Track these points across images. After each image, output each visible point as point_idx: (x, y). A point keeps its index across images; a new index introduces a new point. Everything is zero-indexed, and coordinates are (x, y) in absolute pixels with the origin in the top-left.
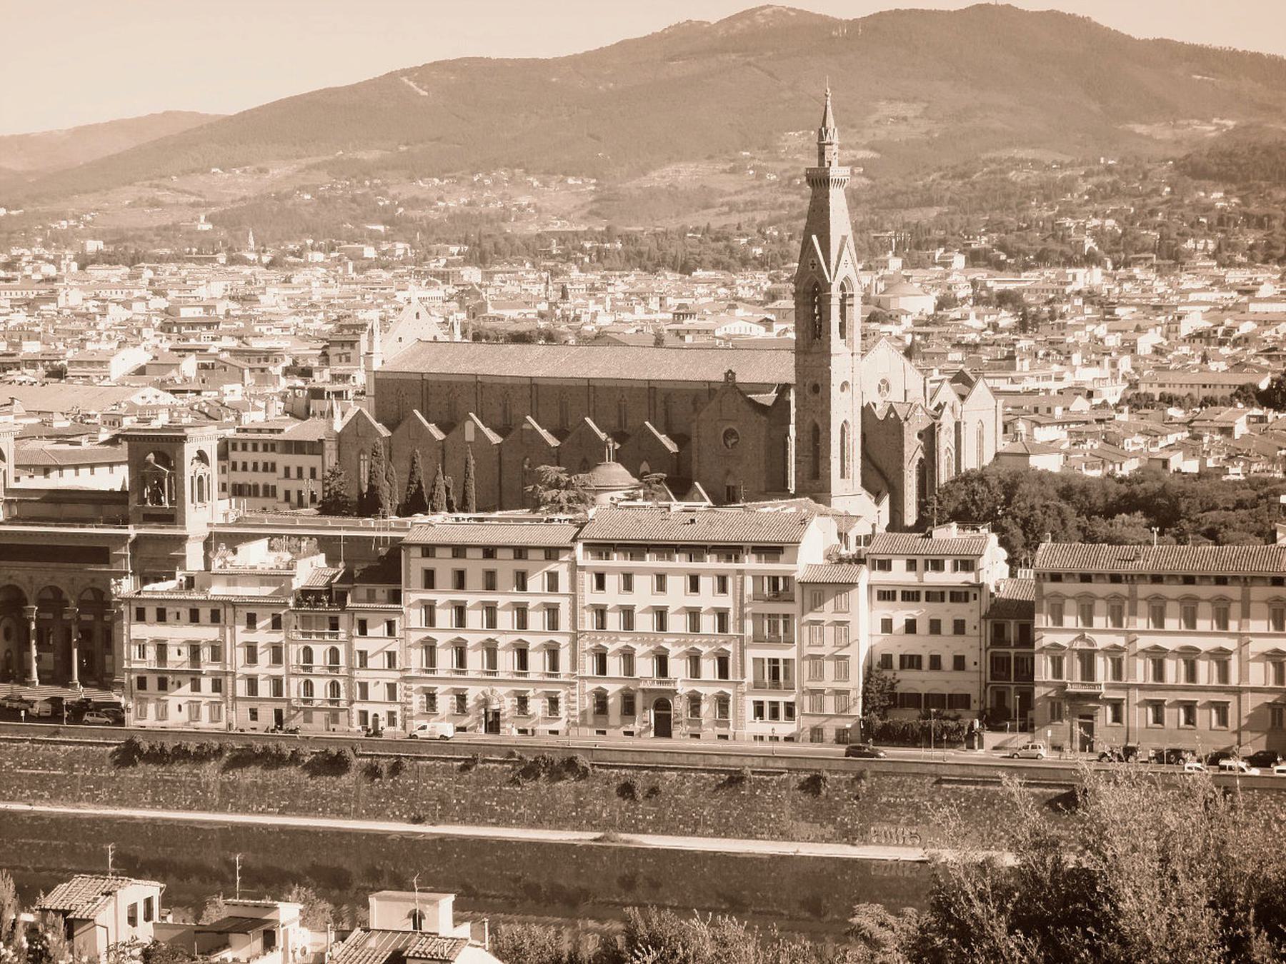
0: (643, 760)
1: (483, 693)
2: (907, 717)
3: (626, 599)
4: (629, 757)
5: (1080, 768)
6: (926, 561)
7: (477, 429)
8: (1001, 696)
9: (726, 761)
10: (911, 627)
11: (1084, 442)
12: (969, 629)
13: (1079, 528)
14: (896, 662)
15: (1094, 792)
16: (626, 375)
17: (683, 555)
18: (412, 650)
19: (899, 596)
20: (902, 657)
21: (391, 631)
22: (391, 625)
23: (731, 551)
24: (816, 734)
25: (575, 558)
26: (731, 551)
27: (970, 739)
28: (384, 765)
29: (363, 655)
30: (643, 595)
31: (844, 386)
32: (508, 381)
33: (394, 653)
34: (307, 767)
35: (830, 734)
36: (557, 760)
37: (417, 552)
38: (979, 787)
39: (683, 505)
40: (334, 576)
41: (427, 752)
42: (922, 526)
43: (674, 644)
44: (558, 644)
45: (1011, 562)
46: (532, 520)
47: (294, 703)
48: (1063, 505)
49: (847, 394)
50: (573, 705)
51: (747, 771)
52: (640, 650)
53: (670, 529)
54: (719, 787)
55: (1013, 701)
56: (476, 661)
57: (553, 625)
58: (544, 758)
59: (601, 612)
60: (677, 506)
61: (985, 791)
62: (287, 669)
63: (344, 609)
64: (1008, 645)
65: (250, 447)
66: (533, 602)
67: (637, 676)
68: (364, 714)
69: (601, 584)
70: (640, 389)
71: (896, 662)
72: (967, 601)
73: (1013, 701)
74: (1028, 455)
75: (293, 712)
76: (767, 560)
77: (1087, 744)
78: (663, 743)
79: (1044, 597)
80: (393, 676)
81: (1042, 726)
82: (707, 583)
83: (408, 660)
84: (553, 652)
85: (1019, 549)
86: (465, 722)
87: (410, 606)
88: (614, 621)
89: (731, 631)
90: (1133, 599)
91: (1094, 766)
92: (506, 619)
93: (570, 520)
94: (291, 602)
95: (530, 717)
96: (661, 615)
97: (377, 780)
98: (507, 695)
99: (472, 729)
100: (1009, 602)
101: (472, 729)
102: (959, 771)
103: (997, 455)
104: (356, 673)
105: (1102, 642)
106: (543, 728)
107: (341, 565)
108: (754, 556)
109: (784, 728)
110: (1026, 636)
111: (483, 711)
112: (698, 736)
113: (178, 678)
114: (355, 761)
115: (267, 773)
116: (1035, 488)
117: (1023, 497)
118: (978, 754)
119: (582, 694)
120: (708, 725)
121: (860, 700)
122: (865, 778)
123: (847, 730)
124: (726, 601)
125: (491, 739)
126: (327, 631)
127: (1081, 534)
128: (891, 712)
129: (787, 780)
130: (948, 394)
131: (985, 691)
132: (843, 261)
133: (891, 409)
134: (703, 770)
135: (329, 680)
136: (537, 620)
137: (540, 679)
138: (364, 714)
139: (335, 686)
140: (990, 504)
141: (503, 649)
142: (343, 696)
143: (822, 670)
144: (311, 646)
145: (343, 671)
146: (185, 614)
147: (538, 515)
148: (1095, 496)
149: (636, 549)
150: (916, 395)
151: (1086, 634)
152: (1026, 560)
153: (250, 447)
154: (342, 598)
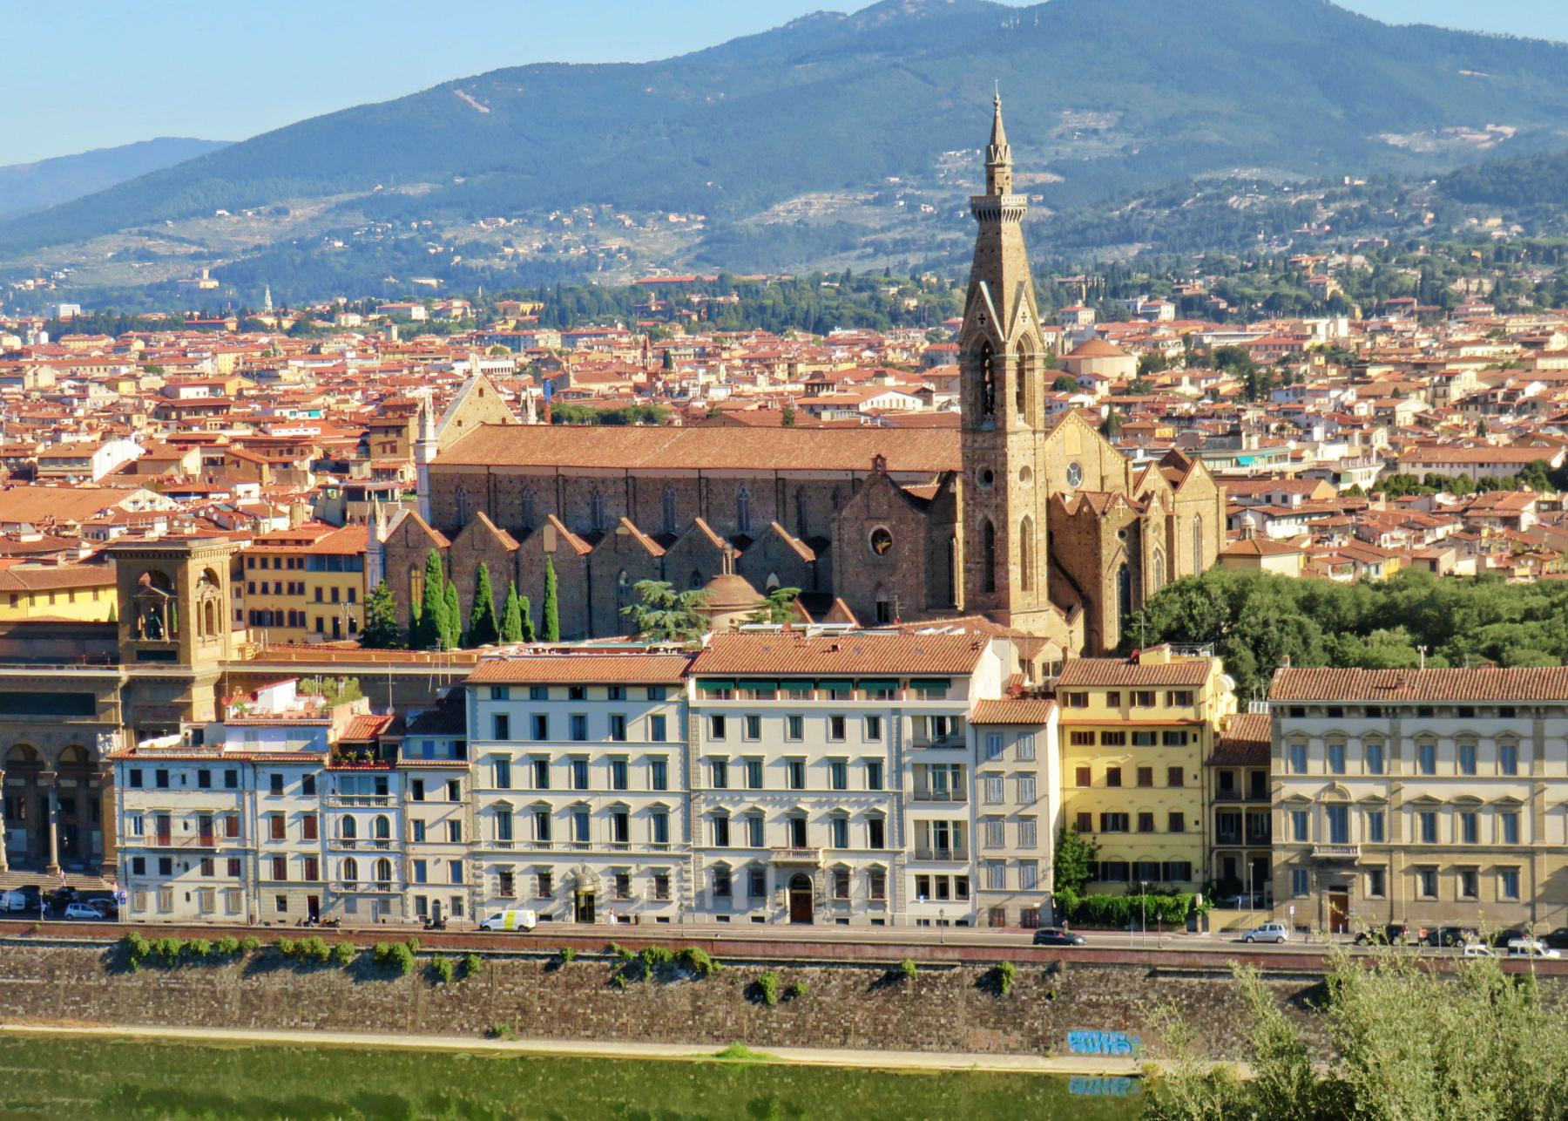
0: (778, 953)
1: (573, 871)
2: (1111, 894)
3: (752, 749)
4: (759, 949)
5: (1331, 953)
6: (1132, 694)
7: (560, 536)
8: (1229, 864)
9: (883, 953)
10: (1114, 777)
11: (1330, 539)
12: (1188, 779)
13: (1325, 648)
14: (1096, 823)
15: (1350, 984)
16: (746, 463)
17: (824, 692)
18: (481, 819)
19: (1098, 738)
20: (1104, 817)
21: (454, 795)
22: (454, 787)
23: (884, 685)
24: (997, 917)
25: (685, 700)
26: (884, 685)
27: (1192, 920)
28: (448, 965)
29: (419, 824)
30: (773, 743)
31: (1025, 473)
32: (598, 474)
33: (459, 822)
34: (350, 969)
35: (1013, 915)
36: (668, 954)
37: (485, 693)
38: (1204, 980)
39: (822, 627)
40: (381, 725)
41: (503, 945)
42: (1127, 649)
43: (814, 805)
44: (666, 808)
45: (1241, 693)
46: (630, 650)
47: (333, 888)
48: (1304, 619)
49: (1028, 484)
50: (686, 885)
51: (909, 965)
52: (770, 812)
53: (805, 658)
54: (874, 985)
55: (1246, 870)
56: (562, 830)
57: (660, 783)
58: (651, 953)
59: (720, 765)
60: (814, 629)
61: (1211, 985)
62: (323, 845)
63: (393, 766)
64: (1238, 799)
65: (271, 563)
66: (633, 754)
67: (767, 846)
68: (421, 901)
69: (719, 729)
70: (764, 481)
71: (1096, 823)
72: (1184, 742)
73: (1246, 870)
74: (1258, 556)
75: (331, 900)
76: (931, 696)
77: (1340, 923)
78: (802, 931)
79: (1282, 737)
80: (457, 852)
81: (1282, 901)
82: (853, 727)
83: (476, 831)
84: (660, 817)
85: (1250, 676)
86: (551, 908)
87: (477, 762)
88: (737, 777)
89: (886, 788)
90: (1395, 736)
91: (1349, 950)
92: (600, 777)
93: (679, 650)
94: (327, 760)
95: (632, 901)
96: (797, 768)
97: (440, 984)
98: (603, 873)
99: (558, 917)
100: (1238, 743)
101: (558, 917)
102: (1178, 960)
103: (1220, 557)
104: (410, 849)
105: (1356, 792)
106: (649, 915)
107: (390, 711)
108: (913, 692)
109: (955, 909)
110: (1261, 787)
111: (572, 895)
112: (846, 921)
113: (185, 858)
114: (411, 961)
115: (300, 978)
116: (1269, 598)
117: (1254, 611)
118: (1202, 939)
119: (699, 869)
120: (858, 907)
121: (1051, 873)
122: (1058, 971)
123: (1035, 911)
124: (879, 750)
125: (583, 929)
126: (373, 795)
127: (1327, 657)
128: (1089, 886)
129: (960, 975)
130: (1155, 480)
131: (1210, 858)
132: (1020, 313)
133: (1085, 500)
134: (854, 965)
135: (376, 858)
136: (639, 777)
137: (645, 852)
138: (421, 901)
139: (384, 866)
140: (1211, 620)
141: (597, 814)
142: (394, 878)
143: (1001, 835)
144: (353, 815)
145: (394, 846)
146: (193, 777)
147: (638, 644)
148: (1344, 608)
149: (764, 684)
150: (1116, 481)
151: (1338, 783)
152: (1259, 690)
153: (271, 563)
154: (392, 751)
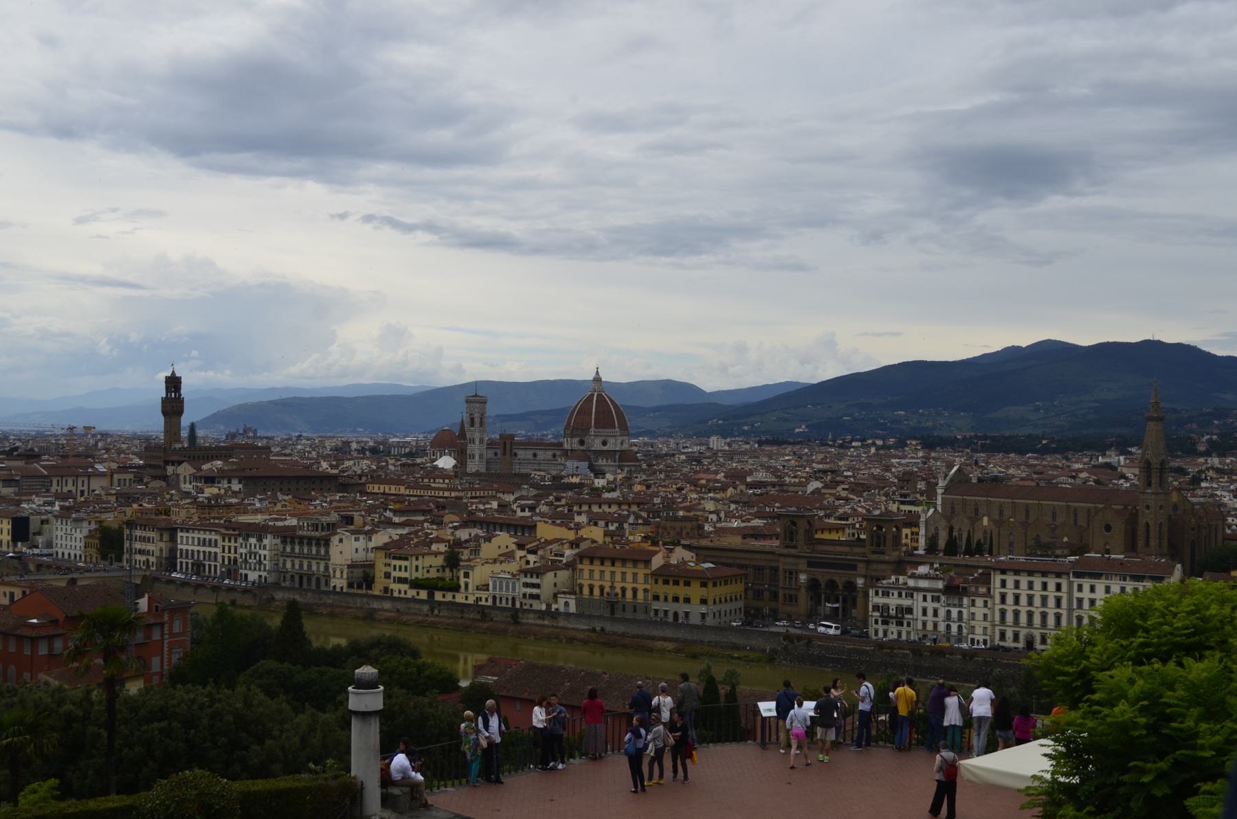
3: (1092, 596)
68: (973, 640)
69: (1080, 588)
80: (987, 624)
88: (1086, 605)
113: (891, 620)
139: (960, 627)
146: (896, 593)
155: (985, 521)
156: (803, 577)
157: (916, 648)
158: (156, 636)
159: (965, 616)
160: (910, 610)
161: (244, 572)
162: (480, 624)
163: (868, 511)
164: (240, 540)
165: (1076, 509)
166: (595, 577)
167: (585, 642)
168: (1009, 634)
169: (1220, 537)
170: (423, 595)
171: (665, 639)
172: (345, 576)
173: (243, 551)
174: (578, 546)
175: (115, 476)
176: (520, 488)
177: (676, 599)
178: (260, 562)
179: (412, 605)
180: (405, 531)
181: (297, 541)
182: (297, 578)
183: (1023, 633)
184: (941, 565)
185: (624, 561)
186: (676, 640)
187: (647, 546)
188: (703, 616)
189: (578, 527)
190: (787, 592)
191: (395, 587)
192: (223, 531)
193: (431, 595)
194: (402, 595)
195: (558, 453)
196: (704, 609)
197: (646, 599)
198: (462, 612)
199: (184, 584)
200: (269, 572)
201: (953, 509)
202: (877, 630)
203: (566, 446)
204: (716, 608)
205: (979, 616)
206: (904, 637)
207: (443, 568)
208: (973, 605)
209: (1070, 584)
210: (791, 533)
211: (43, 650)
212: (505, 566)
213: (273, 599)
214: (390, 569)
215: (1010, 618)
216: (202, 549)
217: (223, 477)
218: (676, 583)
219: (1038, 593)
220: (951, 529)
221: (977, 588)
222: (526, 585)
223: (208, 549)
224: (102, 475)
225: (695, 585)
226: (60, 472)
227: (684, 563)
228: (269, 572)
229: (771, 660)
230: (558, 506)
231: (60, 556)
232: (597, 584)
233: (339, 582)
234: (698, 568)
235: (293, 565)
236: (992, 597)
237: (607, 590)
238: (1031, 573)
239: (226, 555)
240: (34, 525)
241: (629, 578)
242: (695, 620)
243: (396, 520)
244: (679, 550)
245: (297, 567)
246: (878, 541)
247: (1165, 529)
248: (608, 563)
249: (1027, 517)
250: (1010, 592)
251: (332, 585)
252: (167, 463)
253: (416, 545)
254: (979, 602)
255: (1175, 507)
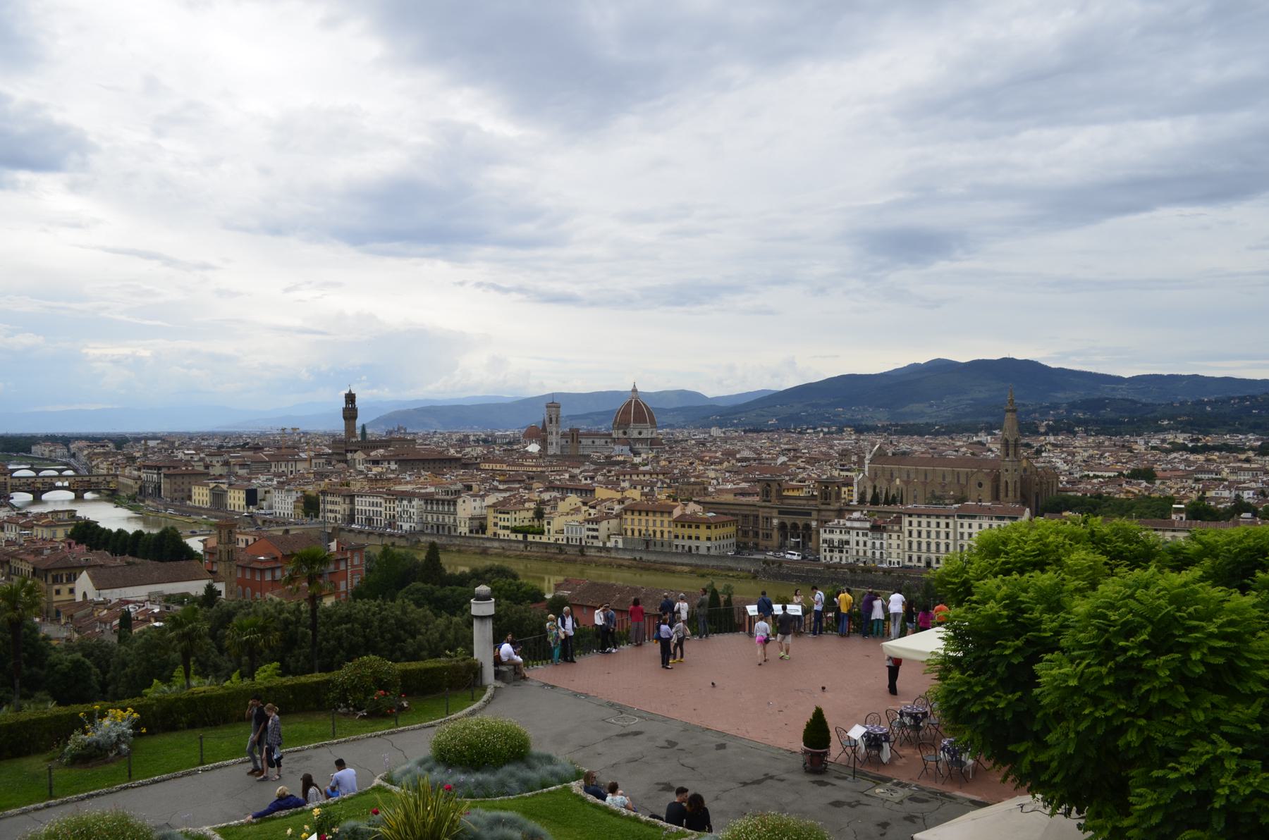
3: (970, 531)
68: (890, 562)
69: (962, 526)
80: (900, 551)
84: (947, 546)
88: (966, 536)
139: (881, 553)
146: (838, 531)
155: (898, 481)
156: (775, 522)
157: (852, 568)
158: (342, 567)
159: (885, 546)
160: (847, 543)
161: (400, 523)
162: (559, 556)
163: (819, 476)
164: (397, 502)
165: (958, 473)
166: (635, 523)
167: (629, 567)
168: (915, 558)
169: (1055, 490)
170: (520, 537)
171: (683, 565)
172: (467, 525)
173: (399, 509)
174: (623, 503)
175: (313, 461)
176: (584, 465)
177: (690, 538)
178: (410, 517)
179: (512, 544)
180: (507, 494)
181: (435, 502)
182: (435, 528)
183: (924, 556)
184: (868, 511)
185: (654, 512)
186: (690, 565)
187: (670, 502)
188: (709, 548)
189: (623, 490)
190: (765, 531)
191: (501, 532)
192: (385, 496)
193: (525, 537)
194: (506, 538)
195: (609, 440)
196: (709, 544)
197: (669, 537)
198: (546, 548)
199: (360, 532)
200: (417, 523)
201: (876, 473)
202: (825, 556)
203: (614, 436)
204: (717, 543)
205: (895, 546)
206: (844, 562)
207: (533, 519)
208: (890, 538)
209: (955, 523)
210: (767, 492)
211: (268, 577)
212: (574, 517)
213: (419, 541)
214: (498, 520)
215: (915, 546)
216: (371, 508)
217: (385, 460)
218: (690, 527)
219: (933, 529)
220: (875, 487)
221: (893, 527)
222: (589, 530)
223: (375, 509)
224: (305, 460)
225: (703, 527)
226: (278, 459)
227: (695, 513)
228: (417, 523)
229: (755, 577)
230: (609, 476)
231: (278, 514)
232: (636, 528)
233: (464, 529)
234: (704, 516)
235: (433, 519)
236: (903, 533)
237: (643, 532)
238: (928, 516)
239: (388, 512)
240: (260, 495)
241: (658, 523)
242: (703, 551)
243: (501, 487)
244: (691, 505)
245: (435, 520)
246: (826, 496)
247: (1018, 485)
248: (644, 514)
249: (926, 478)
250: (915, 529)
251: (459, 531)
252: (347, 451)
253: (515, 504)
254: (894, 536)
255: (1025, 470)
